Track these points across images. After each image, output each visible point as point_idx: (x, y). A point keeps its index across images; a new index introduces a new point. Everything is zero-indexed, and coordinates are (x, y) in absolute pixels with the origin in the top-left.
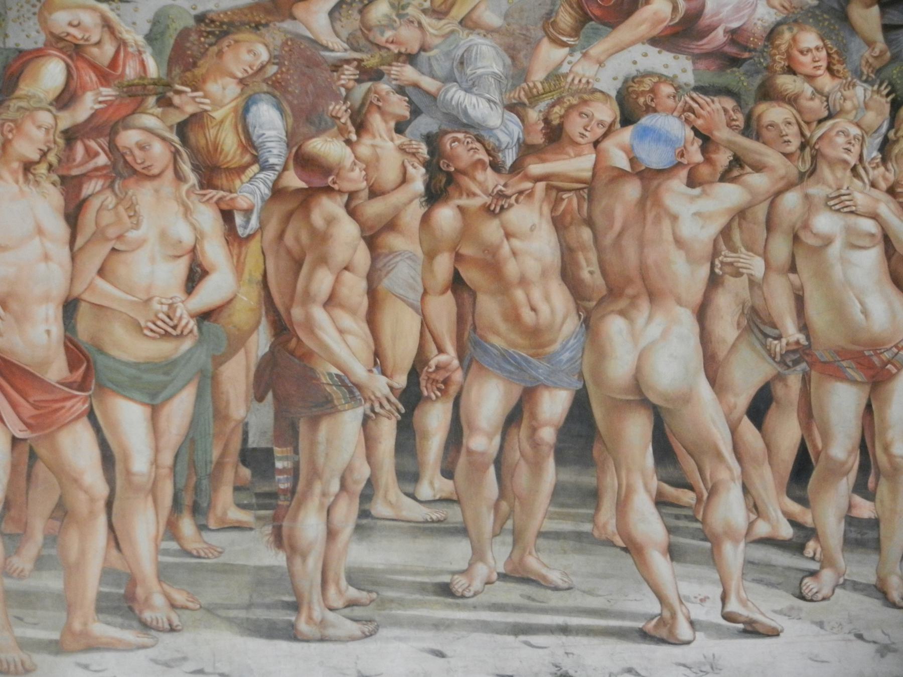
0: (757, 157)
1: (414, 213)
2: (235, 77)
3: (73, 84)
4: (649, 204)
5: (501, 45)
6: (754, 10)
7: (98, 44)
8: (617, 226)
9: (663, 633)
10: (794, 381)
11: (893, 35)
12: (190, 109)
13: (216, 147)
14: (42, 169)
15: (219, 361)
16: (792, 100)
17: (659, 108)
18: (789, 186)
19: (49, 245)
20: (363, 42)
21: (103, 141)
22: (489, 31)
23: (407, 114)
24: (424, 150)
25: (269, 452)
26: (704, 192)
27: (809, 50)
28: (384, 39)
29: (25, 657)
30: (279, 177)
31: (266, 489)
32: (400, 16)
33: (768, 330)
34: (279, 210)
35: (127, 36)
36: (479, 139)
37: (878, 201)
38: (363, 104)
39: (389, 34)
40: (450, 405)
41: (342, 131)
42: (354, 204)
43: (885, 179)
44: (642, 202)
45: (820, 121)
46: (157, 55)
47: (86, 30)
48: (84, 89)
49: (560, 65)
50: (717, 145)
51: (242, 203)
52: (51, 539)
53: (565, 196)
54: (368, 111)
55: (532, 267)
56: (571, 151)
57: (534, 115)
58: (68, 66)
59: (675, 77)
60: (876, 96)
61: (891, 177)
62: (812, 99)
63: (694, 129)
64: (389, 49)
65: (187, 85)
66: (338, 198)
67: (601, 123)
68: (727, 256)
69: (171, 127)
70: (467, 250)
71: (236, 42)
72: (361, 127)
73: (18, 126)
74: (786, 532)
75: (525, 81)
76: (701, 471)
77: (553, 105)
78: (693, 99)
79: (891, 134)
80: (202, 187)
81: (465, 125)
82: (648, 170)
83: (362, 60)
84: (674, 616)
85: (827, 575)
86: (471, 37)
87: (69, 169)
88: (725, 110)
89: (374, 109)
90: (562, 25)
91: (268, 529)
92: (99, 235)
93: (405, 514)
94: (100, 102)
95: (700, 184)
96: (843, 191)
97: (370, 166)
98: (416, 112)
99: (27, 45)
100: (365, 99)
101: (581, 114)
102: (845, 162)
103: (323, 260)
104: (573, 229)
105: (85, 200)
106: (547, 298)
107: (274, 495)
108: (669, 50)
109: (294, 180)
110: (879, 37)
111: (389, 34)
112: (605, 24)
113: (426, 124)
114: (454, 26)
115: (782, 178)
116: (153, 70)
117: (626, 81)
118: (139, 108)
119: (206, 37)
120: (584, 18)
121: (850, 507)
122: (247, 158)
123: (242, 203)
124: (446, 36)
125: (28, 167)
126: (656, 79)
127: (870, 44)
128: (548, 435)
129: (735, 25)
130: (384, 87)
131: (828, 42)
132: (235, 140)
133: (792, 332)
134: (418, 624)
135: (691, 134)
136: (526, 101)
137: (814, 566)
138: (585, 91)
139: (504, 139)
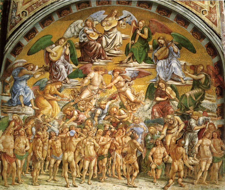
1: (48, 140)
3: (15, 125)
8: (67, 143)
9: (67, 186)
10: (83, 160)
11: (98, 121)
12: (26, 128)
15: (28, 156)
16: (87, 129)
18: (85, 139)
19: (12, 143)
21: (18, 131)
22: (57, 120)
23: (48, 129)
24: (49, 133)
25: (32, 166)
26: (76, 139)
29: (8, 185)
31: (31, 170)
33: (81, 155)
34: (34, 140)
37: (94, 140)
40: (49, 162)
41: (41, 131)
44: (70, 140)
46: (23, 121)
50: (78, 134)
52: (11, 174)
55: (58, 147)
57: (60, 130)
67: (67, 131)
68: (78, 146)
70: (52, 145)
72: (43, 131)
74: (80, 176)
76: (72, 170)
77: (62, 129)
82: (71, 136)
84: (68, 184)
85: (83, 181)
91: (31, 174)
92: (17, 142)
93: (44, 173)
97: (44, 135)
98: (49, 129)
99: (11, 120)
101: (65, 130)
103: (38, 145)
106: (60, 150)
107: (32, 171)
109: (36, 137)
110: (97, 121)
111: (47, 120)
113: (49, 130)
120: (67, 118)
121: (86, 174)
123: (31, 139)
125: (10, 134)
127: (96, 122)
128: (58, 165)
130: (45, 126)
133: (83, 155)
134: (44, 184)
137: (82, 180)
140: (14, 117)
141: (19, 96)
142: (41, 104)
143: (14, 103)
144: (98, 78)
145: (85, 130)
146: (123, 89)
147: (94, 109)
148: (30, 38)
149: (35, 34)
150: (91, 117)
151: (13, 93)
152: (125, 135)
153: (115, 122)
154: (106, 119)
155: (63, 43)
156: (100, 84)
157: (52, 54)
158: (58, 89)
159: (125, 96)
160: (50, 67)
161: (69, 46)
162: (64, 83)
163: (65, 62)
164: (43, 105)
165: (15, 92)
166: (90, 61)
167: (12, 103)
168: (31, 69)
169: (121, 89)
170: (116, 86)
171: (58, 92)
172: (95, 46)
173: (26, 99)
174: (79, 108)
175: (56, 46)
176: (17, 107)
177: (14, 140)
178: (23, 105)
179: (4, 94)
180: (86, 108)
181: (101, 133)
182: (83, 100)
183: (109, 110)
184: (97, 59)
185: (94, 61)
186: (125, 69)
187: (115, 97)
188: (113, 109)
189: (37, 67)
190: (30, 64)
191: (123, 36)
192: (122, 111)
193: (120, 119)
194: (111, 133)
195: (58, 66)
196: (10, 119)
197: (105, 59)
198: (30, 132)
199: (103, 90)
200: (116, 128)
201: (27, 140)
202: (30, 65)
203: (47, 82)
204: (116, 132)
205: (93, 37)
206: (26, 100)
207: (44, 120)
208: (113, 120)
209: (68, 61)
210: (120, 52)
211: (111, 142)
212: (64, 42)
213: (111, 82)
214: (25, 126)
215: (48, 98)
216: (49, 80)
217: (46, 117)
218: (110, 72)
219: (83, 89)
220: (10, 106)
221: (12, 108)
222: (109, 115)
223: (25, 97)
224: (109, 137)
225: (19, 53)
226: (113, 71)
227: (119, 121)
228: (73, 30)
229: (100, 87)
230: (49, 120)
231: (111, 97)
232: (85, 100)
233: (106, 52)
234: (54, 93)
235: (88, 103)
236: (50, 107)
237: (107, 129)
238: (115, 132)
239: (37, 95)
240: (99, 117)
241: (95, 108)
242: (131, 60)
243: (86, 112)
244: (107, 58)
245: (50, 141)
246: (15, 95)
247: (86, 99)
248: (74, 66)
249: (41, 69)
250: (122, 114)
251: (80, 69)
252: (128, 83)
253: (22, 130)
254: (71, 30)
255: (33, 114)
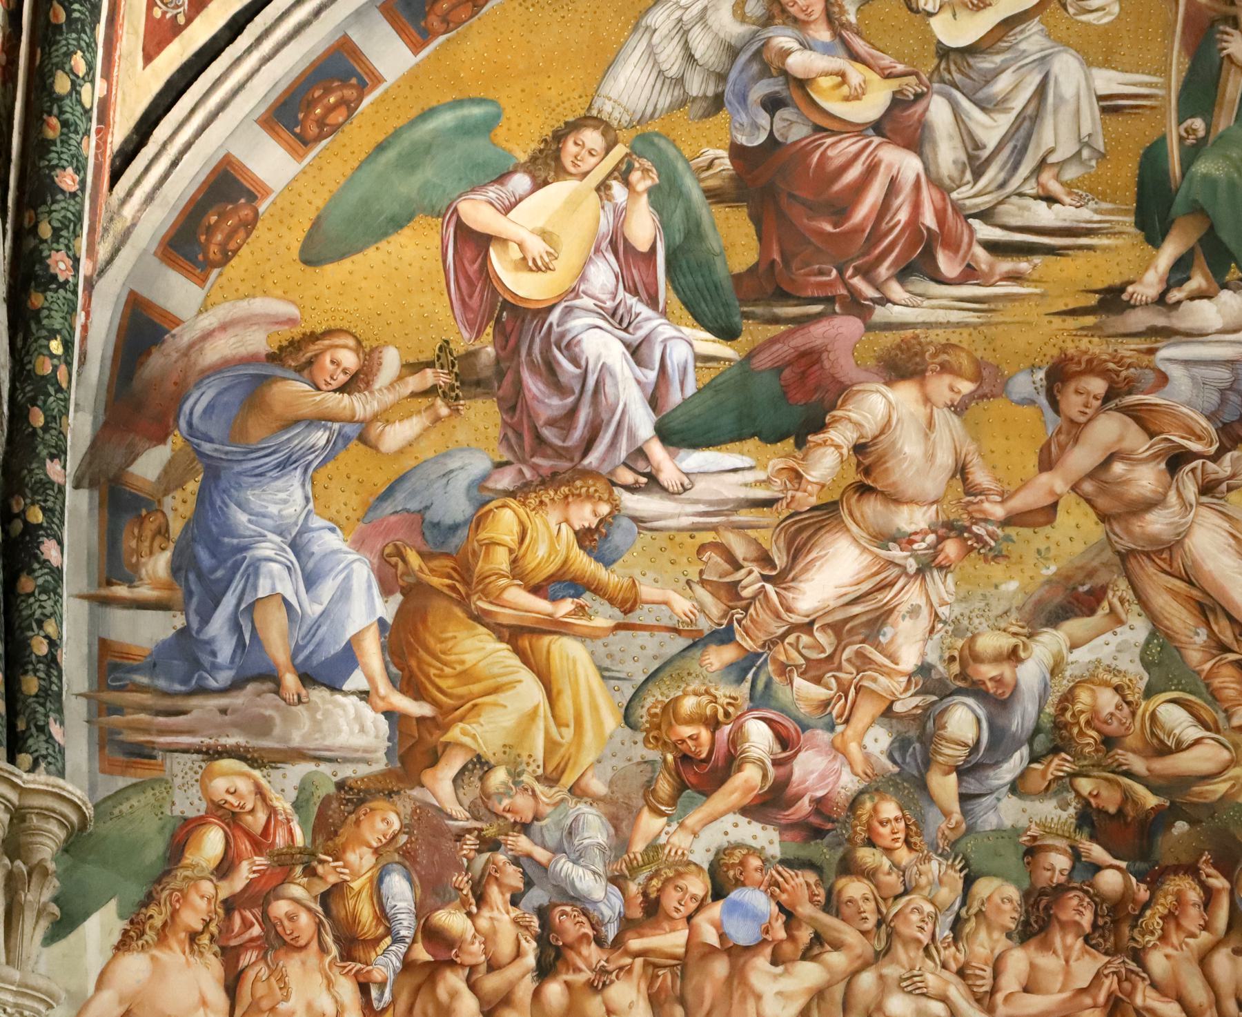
0: (836, 934)
1: (527, 986)
2: (370, 847)
3: (231, 853)
4: (735, 983)
5: (605, 814)
6: (839, 778)
7: (252, 811)
8: (707, 1005)
12: (332, 879)
13: (355, 919)
14: (205, 940)
16: (870, 875)
17: (747, 882)
18: (865, 966)
20: (483, 811)
21: (257, 911)
23: (521, 885)
24: (535, 923)
26: (786, 971)
27: (889, 821)
28: (501, 808)
30: (409, 948)
32: (515, 783)
35: (276, 803)
36: (585, 913)
37: (947, 982)
38: (482, 876)
39: (506, 802)
41: (464, 903)
42: (474, 977)
43: (955, 959)
44: (729, 980)
45: (897, 897)
46: (302, 824)
47: (241, 797)
48: (241, 859)
49: (659, 835)
51: (377, 976)
53: (660, 973)
54: (487, 882)
56: (666, 926)
57: (634, 888)
58: (226, 833)
59: (763, 848)
60: (950, 872)
61: (961, 957)
62: (889, 874)
63: (778, 904)
64: (506, 819)
65: (329, 855)
66: (460, 971)
67: (693, 897)
69: (315, 898)
71: (372, 810)
72: (481, 899)
73: (185, 896)
75: (627, 852)
77: (650, 879)
78: (779, 873)
79: (963, 912)
80: (343, 959)
81: (572, 898)
82: (736, 946)
83: (482, 830)
86: (579, 806)
87: (229, 939)
88: (808, 885)
89: (492, 881)
90: (661, 794)
94: (254, 872)
95: (783, 963)
96: (916, 972)
97: (489, 939)
98: (529, 884)
99: (191, 813)
100: (484, 870)
102: (919, 941)
104: (667, 1006)
105: (243, 971)
108: (758, 821)
109: (422, 954)
110: (955, 807)
111: (506, 802)
112: (699, 792)
113: (537, 896)
114: (564, 794)
115: (859, 957)
116: (300, 840)
117: (717, 854)
118: (287, 879)
119: (346, 805)
122: (381, 930)
124: (557, 805)
125: (193, 937)
126: (745, 852)
129: (820, 794)
130: (501, 858)
131: (907, 812)
132: (371, 911)
135: (776, 909)
136: (627, 872)
138: (680, 863)
139: (607, 913)
140: (219, 785)
141: (251, 607)
142: (447, 670)
143: (215, 667)
144: (926, 435)
145: (855, 889)
146: (1156, 523)
147: (917, 700)
148: (313, 130)
149: (350, 93)
150: (896, 769)
151: (200, 576)
152: (1230, 926)
153: (1120, 812)
154: (1039, 784)
155: (593, 160)
156: (949, 486)
157: (515, 253)
158: (584, 537)
159: (1178, 583)
160: (498, 360)
161: (649, 183)
162: (632, 489)
163: (629, 311)
164: (466, 676)
165: (220, 573)
166: (843, 291)
167: (197, 665)
168: (342, 378)
169: (1137, 526)
170: (1089, 501)
171: (584, 563)
172: (872, 170)
173: (317, 624)
174: (782, 692)
175: (539, 184)
176: (237, 700)
177: (232, 987)
178: (290, 681)
179: (121, 591)
180: (844, 690)
181: (1009, 917)
182: (812, 623)
183: (1050, 710)
184: (904, 274)
185: (876, 295)
186: (1152, 351)
187: (1090, 592)
188: (1084, 697)
189: (391, 360)
190: (328, 333)
191: (1108, 81)
192: (1176, 719)
193: (1161, 782)
194: (1096, 914)
195: (569, 344)
196: (188, 803)
197: (970, 274)
198: (366, 913)
199: (979, 538)
200: (1141, 866)
201: (347, 990)
202: (327, 342)
203: (486, 477)
204: (1147, 905)
205: (847, 99)
206: (316, 639)
207: (482, 807)
208: (1104, 793)
209: (653, 302)
210: (1096, 211)
211: (1110, 995)
212: (608, 150)
213: (1047, 463)
214: (322, 862)
215: (506, 616)
216: (499, 465)
217: (499, 777)
218: (1027, 383)
219: (805, 535)
220: (178, 687)
221: (195, 714)
222: (1055, 750)
223: (309, 612)
224: (1084, 952)
225: (235, 252)
226: (1049, 376)
227: (1151, 801)
228: (670, 58)
229: (954, 513)
230: (523, 803)
231: (1059, 598)
232: (823, 628)
233: (975, 216)
234: (551, 569)
235: (860, 655)
236: (530, 690)
237: (1058, 879)
238: (1134, 901)
239: (405, 592)
240: (963, 772)
241: (923, 691)
242: (1197, 281)
243: (850, 732)
244: (984, 267)
245: (554, 991)
246: (217, 604)
247: (839, 616)
248: (708, 344)
249: (429, 377)
250: (1179, 743)
251: (763, 361)
252: (1193, 470)
253: (296, 901)
254: (651, 52)
255: (381, 754)
